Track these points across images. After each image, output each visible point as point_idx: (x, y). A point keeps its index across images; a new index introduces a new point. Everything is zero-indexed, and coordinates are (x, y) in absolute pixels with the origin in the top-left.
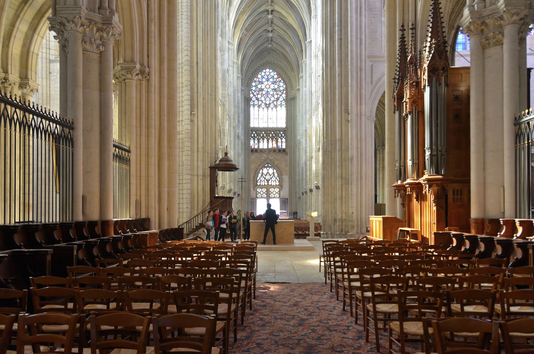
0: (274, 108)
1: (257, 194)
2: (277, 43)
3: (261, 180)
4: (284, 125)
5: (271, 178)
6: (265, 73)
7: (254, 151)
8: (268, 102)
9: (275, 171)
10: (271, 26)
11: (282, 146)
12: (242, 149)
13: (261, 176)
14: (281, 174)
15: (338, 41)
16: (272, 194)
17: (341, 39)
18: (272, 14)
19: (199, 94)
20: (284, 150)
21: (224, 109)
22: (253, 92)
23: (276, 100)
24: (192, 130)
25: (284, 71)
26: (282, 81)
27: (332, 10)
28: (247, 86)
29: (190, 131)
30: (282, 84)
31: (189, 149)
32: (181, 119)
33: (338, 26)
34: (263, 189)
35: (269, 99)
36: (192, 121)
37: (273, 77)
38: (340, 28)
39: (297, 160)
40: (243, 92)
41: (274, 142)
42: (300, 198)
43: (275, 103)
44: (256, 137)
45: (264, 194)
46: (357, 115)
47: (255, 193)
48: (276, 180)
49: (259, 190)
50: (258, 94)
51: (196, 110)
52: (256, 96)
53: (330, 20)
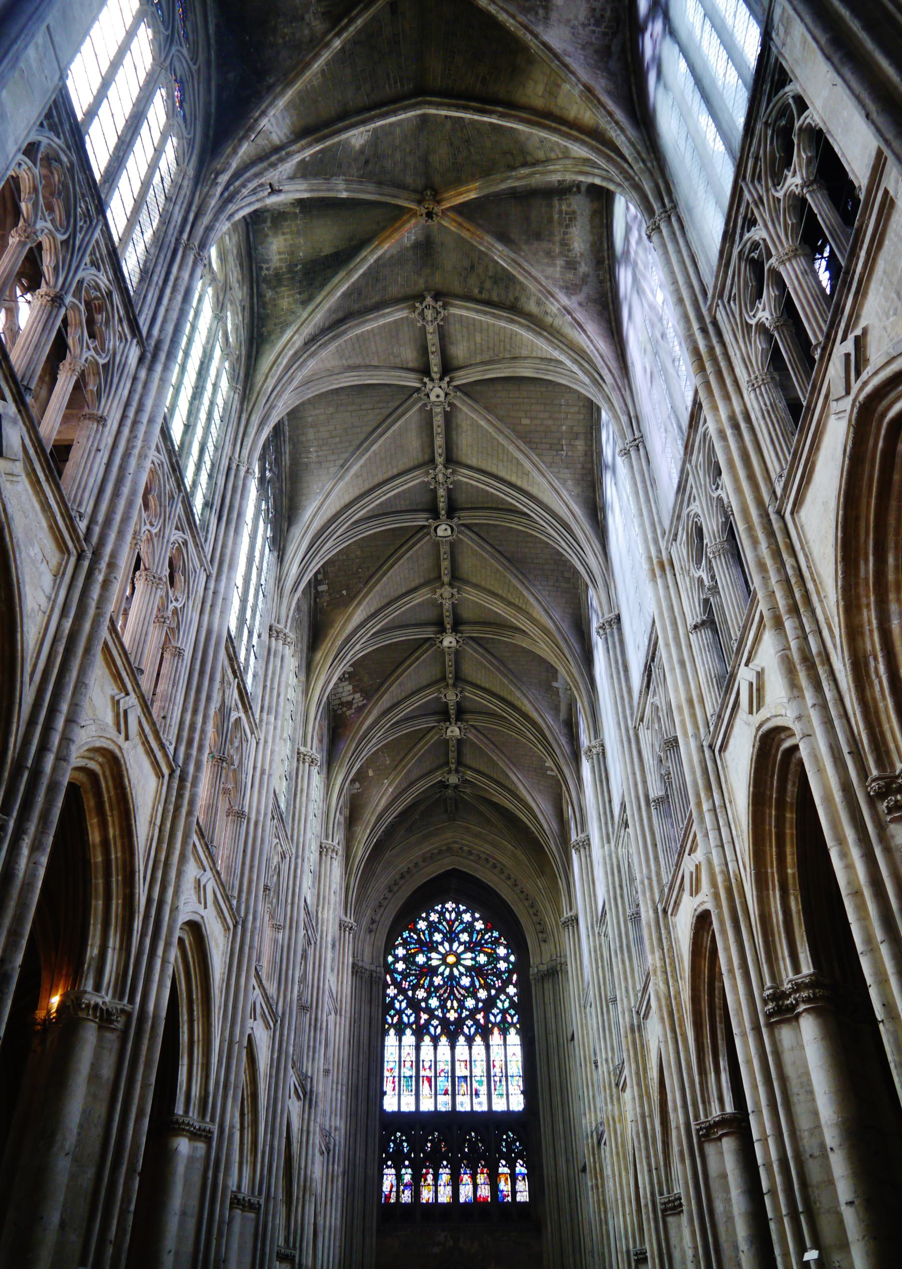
0: (478, 1039)
4: (517, 1104)
6: (441, 914)
8: (452, 1016)
11: (514, 1192)
12: (330, 1178)
18: (455, 629)
22: (399, 978)
23: (482, 1009)
25: (509, 878)
26: (502, 940)
28: (371, 931)
30: (502, 951)
35: (455, 1004)
37: (469, 928)
41: (481, 1179)
43: (480, 1016)
50: (414, 988)
52: (410, 993)
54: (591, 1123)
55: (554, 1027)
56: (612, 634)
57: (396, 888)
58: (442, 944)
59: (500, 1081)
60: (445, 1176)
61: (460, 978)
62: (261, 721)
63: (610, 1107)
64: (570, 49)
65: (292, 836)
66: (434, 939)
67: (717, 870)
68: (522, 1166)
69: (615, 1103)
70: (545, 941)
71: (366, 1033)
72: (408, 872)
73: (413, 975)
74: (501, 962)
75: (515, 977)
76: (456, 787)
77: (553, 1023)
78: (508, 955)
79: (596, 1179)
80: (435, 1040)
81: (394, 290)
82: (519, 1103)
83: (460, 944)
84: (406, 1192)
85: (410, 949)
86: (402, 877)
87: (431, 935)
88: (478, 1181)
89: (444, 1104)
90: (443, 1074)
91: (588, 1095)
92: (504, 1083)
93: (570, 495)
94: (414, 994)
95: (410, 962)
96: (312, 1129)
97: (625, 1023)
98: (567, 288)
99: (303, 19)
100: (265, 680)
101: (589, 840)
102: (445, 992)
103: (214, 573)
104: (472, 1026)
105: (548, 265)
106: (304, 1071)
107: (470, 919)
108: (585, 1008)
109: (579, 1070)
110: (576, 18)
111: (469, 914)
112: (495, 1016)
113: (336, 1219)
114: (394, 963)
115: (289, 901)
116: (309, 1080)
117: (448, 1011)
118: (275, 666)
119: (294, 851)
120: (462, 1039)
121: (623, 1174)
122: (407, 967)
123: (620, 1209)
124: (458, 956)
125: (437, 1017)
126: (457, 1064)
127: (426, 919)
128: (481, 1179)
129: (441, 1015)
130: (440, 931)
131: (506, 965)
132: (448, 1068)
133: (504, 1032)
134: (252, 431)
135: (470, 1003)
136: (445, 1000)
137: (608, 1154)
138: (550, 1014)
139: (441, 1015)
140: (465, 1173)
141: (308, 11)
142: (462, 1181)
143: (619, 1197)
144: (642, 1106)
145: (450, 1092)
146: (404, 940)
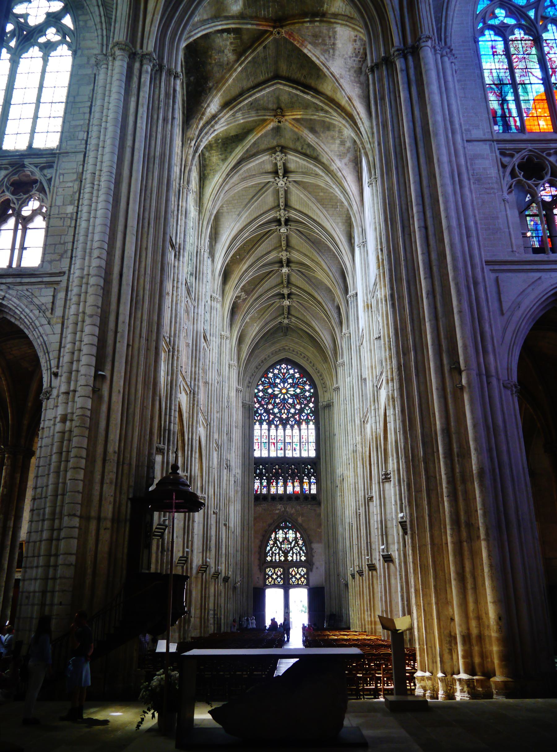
0: (296, 426)
1: (265, 579)
2: (297, 318)
3: (273, 553)
4: (313, 454)
5: (292, 549)
6: (280, 370)
7: (259, 499)
8: (284, 416)
9: (298, 535)
10: (287, 287)
11: (310, 489)
12: (236, 492)
13: (274, 545)
14: (310, 541)
15: (420, 231)
16: (294, 579)
17: (426, 228)
18: (288, 266)
19: (119, 335)
20: (314, 497)
21: (194, 400)
22: (260, 399)
23: (298, 414)
24: (95, 410)
27: (402, 180)
28: (248, 387)
29: (88, 413)
30: (307, 387)
31: (84, 453)
32: (72, 388)
33: (417, 204)
34: (276, 570)
35: (286, 411)
36: (96, 392)
38: (421, 207)
39: (339, 513)
40: (241, 395)
41: (296, 484)
42: (347, 585)
43: (297, 417)
45: (279, 579)
46: (479, 375)
47: (261, 577)
48: (301, 552)
49: (269, 571)
50: (267, 404)
51: (108, 367)
52: (265, 406)
53: (400, 197)
56: (354, 301)
57: (259, 367)
58: (280, 384)
60: (281, 483)
62: (210, 340)
64: (343, 73)
67: (374, 431)
71: (248, 431)
75: (313, 399)
78: (310, 389)
80: (277, 426)
81: (263, 147)
86: (262, 362)
88: (295, 485)
89: (280, 454)
92: (307, 445)
93: (340, 231)
98: (340, 155)
99: (223, 52)
100: (211, 322)
103: (196, 305)
105: (332, 144)
110: (347, 53)
112: (304, 417)
114: (258, 393)
118: (214, 314)
122: (264, 395)
124: (287, 390)
125: (278, 417)
126: (286, 437)
128: (296, 484)
132: (283, 439)
133: (307, 423)
134: (204, 230)
135: (292, 411)
136: (281, 409)
138: (327, 424)
141: (226, 48)
144: (355, 479)
146: (262, 382)
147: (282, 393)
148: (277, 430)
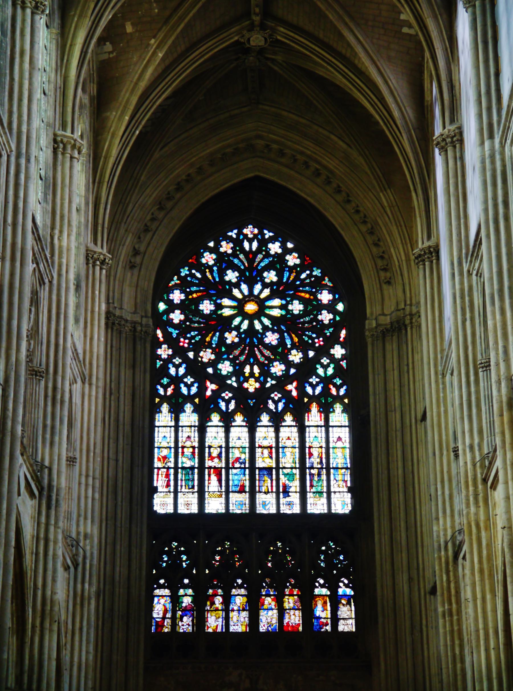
0: (289, 419)
6: (237, 243)
8: (252, 386)
11: (335, 619)
22: (175, 333)
25: (338, 190)
28: (132, 267)
30: (325, 297)
35: (256, 370)
41: (289, 602)
43: (291, 387)
44: (187, 573)
50: (198, 347)
52: (191, 355)
54: (445, 530)
55: (397, 402)
57: (169, 205)
58: (237, 285)
59: (319, 475)
61: (263, 334)
63: (473, 509)
65: (10, 123)
66: (227, 278)
68: (347, 586)
69: (481, 504)
70: (389, 283)
71: (128, 408)
72: (187, 181)
73: (195, 329)
74: (324, 312)
75: (343, 333)
76: (261, 51)
77: (397, 397)
79: (450, 604)
82: (344, 504)
83: (265, 286)
84: (185, 619)
85: (192, 293)
86: (179, 188)
87: (222, 273)
88: (286, 605)
90: (237, 465)
91: (443, 493)
92: (324, 477)
94: (197, 355)
95: (191, 311)
96: (51, 536)
97: (500, 396)
101: (461, 134)
102: (241, 353)
104: (280, 400)
106: (39, 459)
107: (280, 251)
108: (444, 376)
109: (431, 460)
111: (278, 244)
112: (314, 387)
113: (87, 652)
115: (10, 220)
116: (46, 471)
117: (246, 380)
119: (13, 147)
120: (265, 419)
121: (488, 597)
122: (187, 319)
123: (482, 642)
124: (261, 303)
125: (230, 388)
126: (258, 451)
127: (215, 250)
128: (289, 602)
129: (235, 385)
130: (235, 268)
131: (331, 316)
132: (246, 456)
135: (278, 369)
136: (242, 365)
137: (467, 572)
139: (235, 385)
140: (268, 595)
142: (263, 604)
143: (481, 626)
145: (247, 489)
147: (245, 316)
148: (227, 432)
